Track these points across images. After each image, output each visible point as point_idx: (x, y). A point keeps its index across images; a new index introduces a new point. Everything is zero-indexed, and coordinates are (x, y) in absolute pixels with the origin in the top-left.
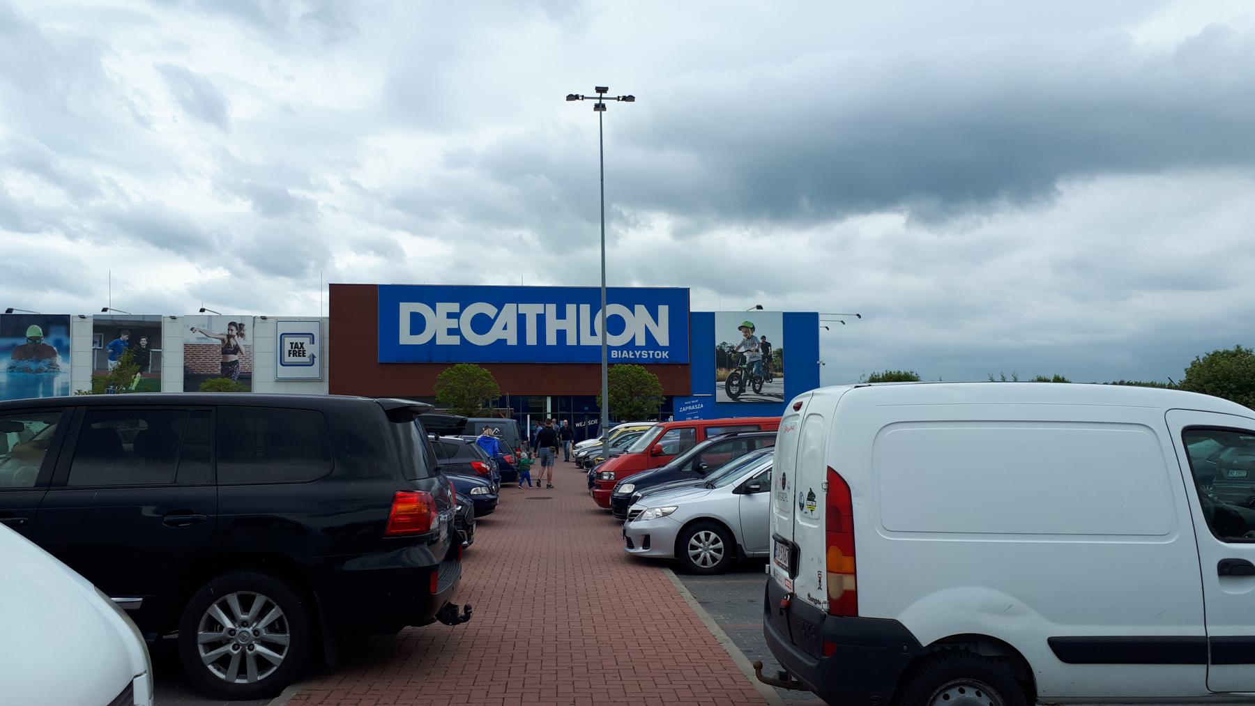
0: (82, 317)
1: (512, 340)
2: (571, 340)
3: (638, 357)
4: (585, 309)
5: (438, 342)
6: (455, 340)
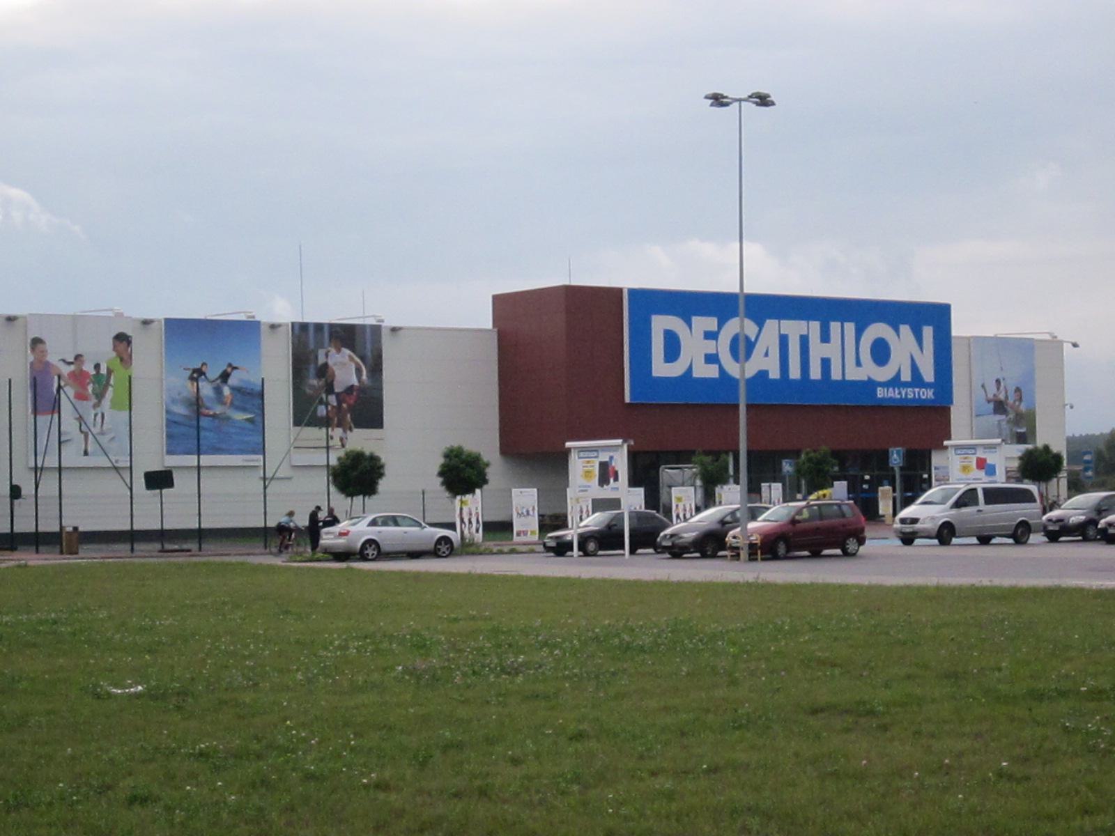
0: (146, 323)
1: (775, 374)
4: (850, 327)
5: (696, 374)
6: (712, 372)
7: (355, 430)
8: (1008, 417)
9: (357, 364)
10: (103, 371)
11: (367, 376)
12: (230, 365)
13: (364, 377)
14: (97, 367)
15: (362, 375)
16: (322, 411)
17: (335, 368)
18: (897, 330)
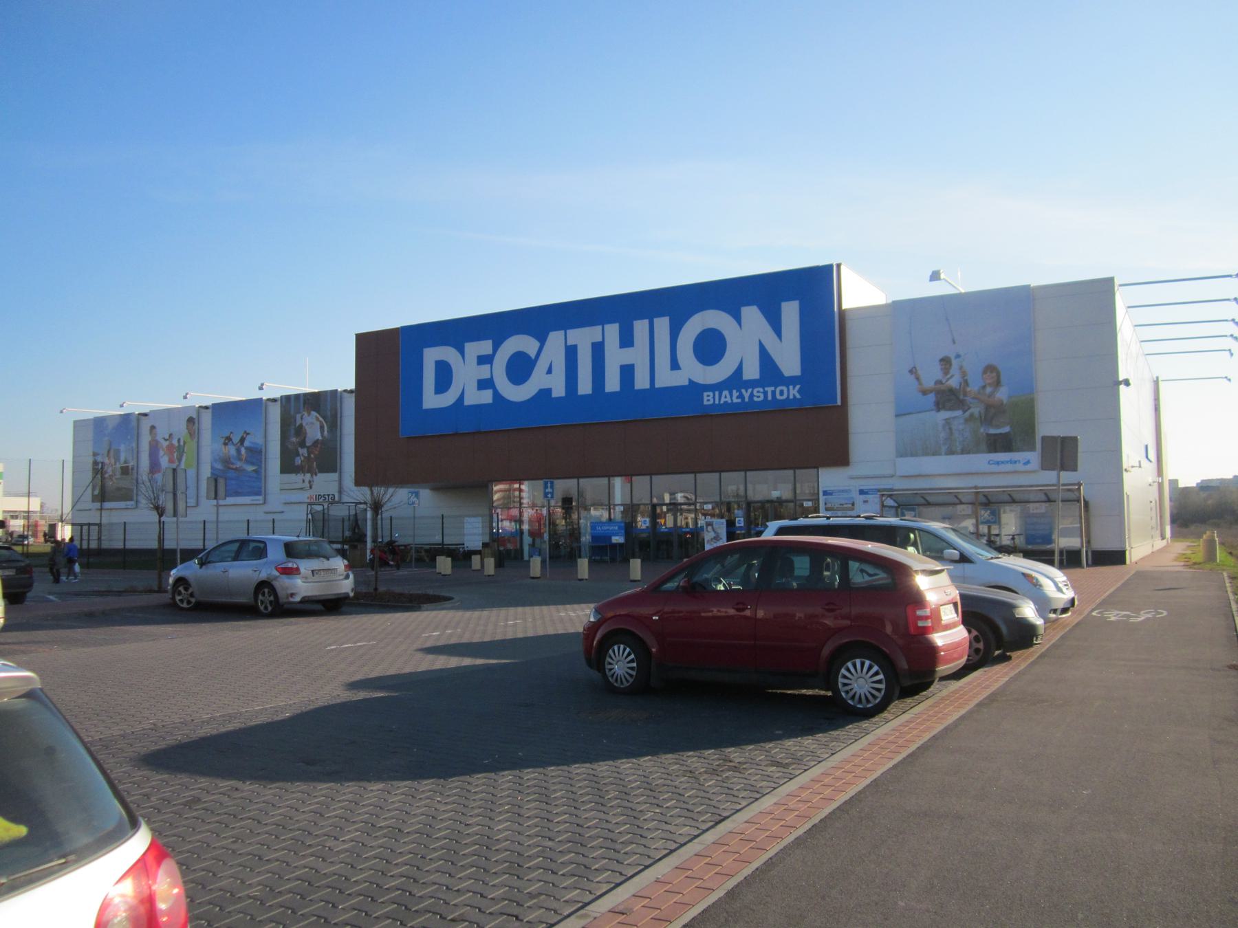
1: (559, 391)
3: (747, 400)
4: (663, 325)
5: (468, 401)
6: (486, 397)
7: (319, 475)
8: (967, 414)
9: (320, 422)
10: (182, 443)
11: (328, 432)
12: (245, 432)
13: (326, 432)
14: (179, 440)
15: (324, 431)
16: (298, 461)
17: (307, 427)
18: (738, 318)
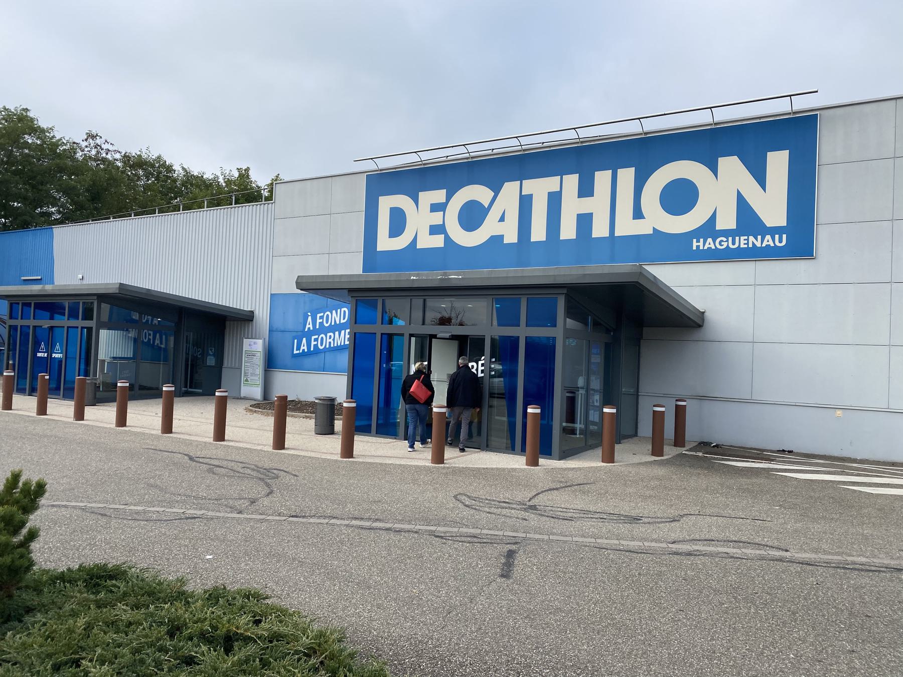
1: (511, 237)
2: (600, 230)
4: (627, 176)
6: (438, 241)
